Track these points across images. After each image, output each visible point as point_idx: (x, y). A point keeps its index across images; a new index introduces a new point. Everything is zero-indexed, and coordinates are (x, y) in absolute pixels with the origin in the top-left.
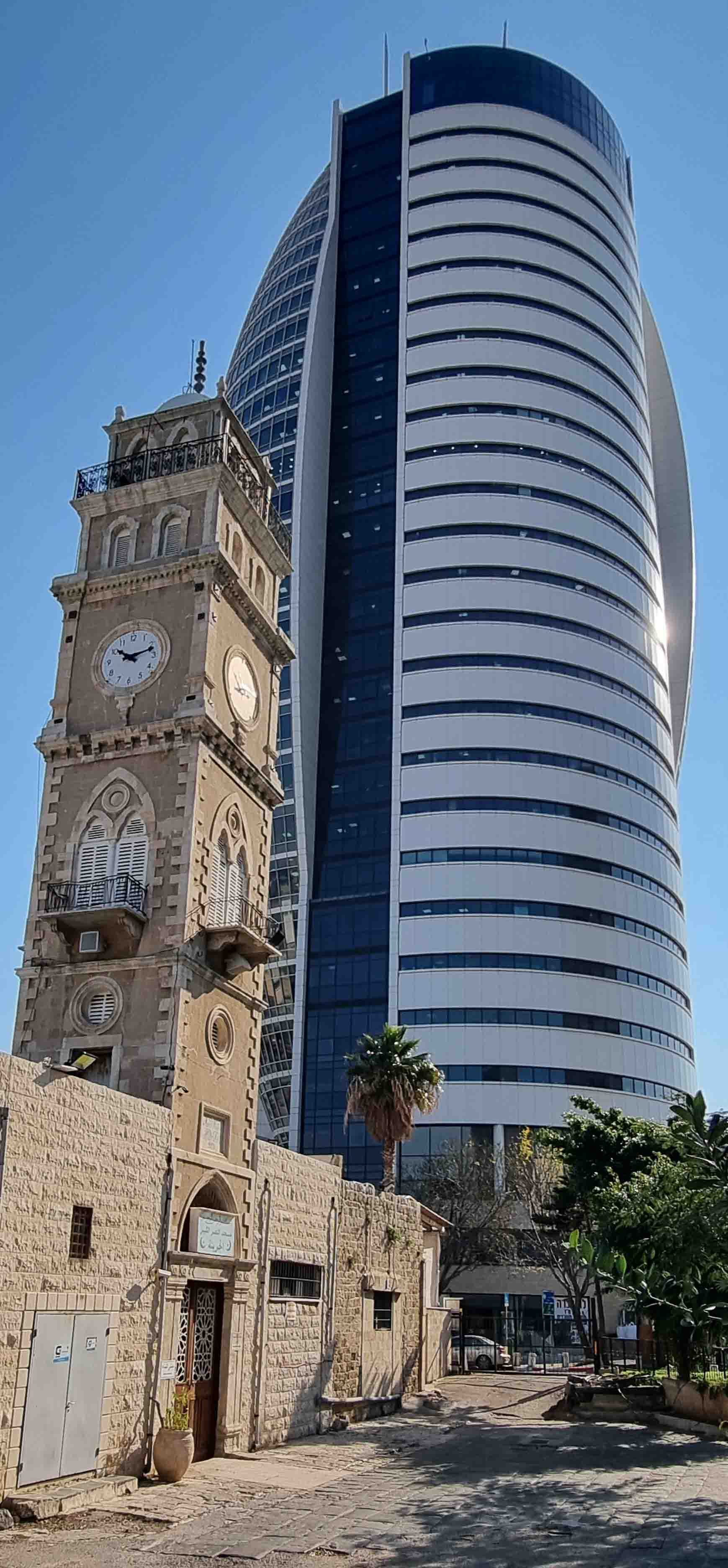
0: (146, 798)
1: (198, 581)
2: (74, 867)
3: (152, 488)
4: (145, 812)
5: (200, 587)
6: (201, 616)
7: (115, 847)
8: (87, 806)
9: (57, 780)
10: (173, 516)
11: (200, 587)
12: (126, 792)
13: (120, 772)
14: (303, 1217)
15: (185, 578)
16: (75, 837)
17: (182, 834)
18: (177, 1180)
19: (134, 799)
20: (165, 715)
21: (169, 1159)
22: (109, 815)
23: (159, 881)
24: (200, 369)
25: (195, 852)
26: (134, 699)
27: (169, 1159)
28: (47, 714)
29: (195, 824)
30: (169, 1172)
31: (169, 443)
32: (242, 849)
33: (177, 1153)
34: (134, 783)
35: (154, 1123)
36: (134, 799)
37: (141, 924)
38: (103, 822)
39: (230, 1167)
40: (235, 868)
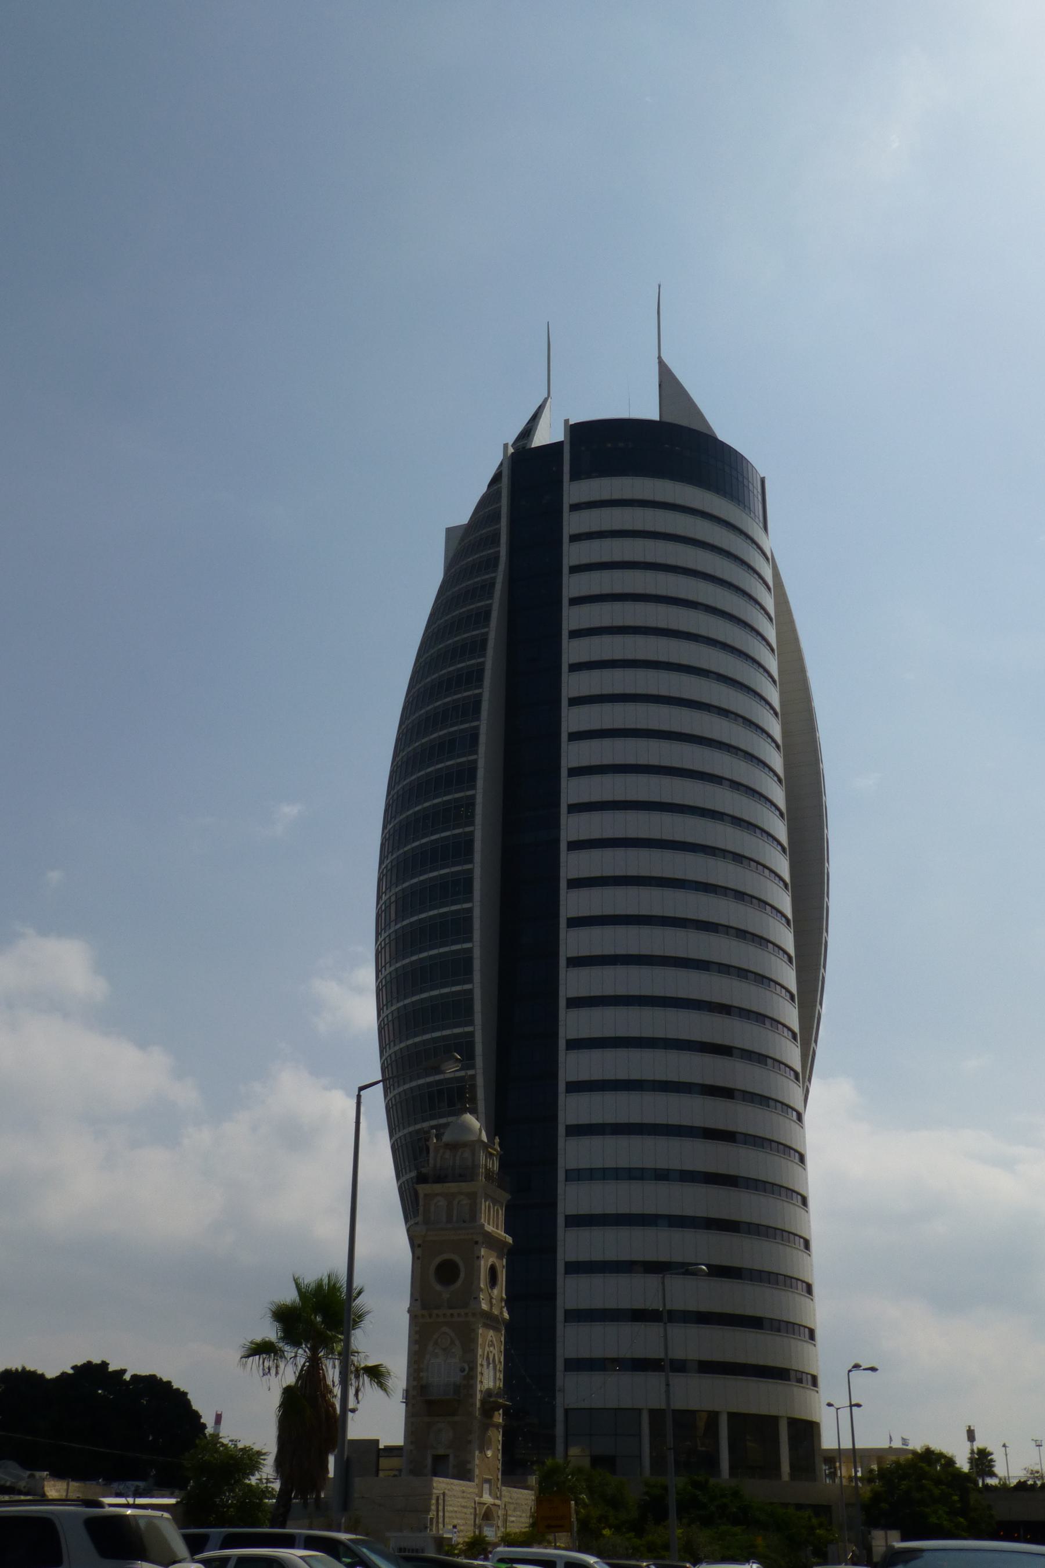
0: (457, 1342)
5: (477, 1243)
6: (478, 1258)
11: (477, 1243)
13: (445, 1329)
35: (471, 1490)
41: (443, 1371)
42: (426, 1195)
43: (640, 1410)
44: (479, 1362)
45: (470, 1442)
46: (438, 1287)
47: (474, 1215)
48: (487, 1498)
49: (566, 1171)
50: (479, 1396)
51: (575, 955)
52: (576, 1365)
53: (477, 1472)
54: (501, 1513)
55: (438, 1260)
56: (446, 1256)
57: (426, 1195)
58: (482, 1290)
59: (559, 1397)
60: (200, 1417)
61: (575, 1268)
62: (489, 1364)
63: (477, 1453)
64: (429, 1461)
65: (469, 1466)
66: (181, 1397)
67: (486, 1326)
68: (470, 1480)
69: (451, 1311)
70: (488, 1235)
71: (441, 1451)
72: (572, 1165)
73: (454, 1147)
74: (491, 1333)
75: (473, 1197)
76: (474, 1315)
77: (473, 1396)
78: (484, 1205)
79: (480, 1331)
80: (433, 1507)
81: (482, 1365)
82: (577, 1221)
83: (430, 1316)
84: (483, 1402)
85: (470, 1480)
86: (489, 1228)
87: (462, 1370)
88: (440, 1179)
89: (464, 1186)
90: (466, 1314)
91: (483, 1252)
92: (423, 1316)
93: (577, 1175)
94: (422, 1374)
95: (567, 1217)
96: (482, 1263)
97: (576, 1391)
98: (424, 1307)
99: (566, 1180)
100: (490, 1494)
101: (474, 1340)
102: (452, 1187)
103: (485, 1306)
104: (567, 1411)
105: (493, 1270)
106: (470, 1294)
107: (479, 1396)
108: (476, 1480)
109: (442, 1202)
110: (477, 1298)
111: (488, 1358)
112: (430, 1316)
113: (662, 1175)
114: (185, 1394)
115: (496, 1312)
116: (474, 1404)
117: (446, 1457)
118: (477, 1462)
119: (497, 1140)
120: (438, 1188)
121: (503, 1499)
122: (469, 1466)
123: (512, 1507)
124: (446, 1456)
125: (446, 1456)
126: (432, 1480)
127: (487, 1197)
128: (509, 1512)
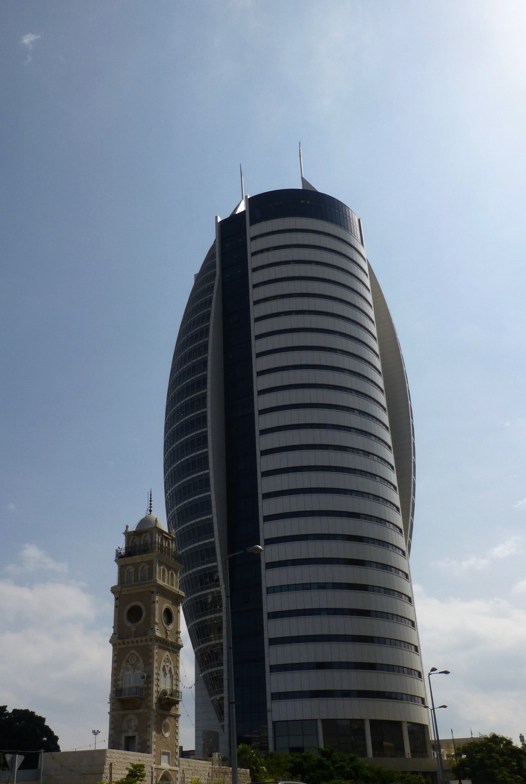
0: (141, 660)
1: (152, 591)
2: (122, 680)
3: (137, 558)
4: (141, 665)
5: (153, 592)
6: (154, 602)
8: (125, 661)
11: (153, 592)
12: (136, 658)
13: (133, 651)
15: (148, 589)
16: (122, 671)
17: (152, 671)
18: (155, 774)
19: (138, 660)
20: (146, 635)
21: (152, 769)
22: (131, 665)
23: (146, 686)
24: (151, 504)
25: (155, 677)
27: (152, 769)
28: (112, 631)
29: (155, 668)
30: (152, 772)
31: (142, 543)
32: (170, 668)
33: (154, 766)
34: (138, 655)
36: (138, 660)
37: (142, 699)
38: (129, 666)
39: (171, 768)
40: (168, 675)
41: (133, 679)
43: (316, 720)
44: (155, 671)
45: (149, 726)
46: (129, 624)
48: (165, 765)
50: (155, 695)
52: (278, 696)
53: (154, 747)
54: (179, 776)
55: (129, 607)
56: (134, 604)
58: (157, 624)
59: (269, 714)
61: (274, 642)
62: (165, 675)
63: (154, 733)
64: (123, 741)
65: (148, 743)
67: (160, 647)
68: (149, 752)
69: (137, 639)
70: (160, 587)
71: (130, 734)
74: (167, 653)
75: (150, 563)
76: (151, 640)
77: (151, 695)
78: (158, 569)
80: (107, 771)
81: (158, 674)
82: (274, 615)
83: (124, 643)
84: (160, 699)
85: (149, 753)
86: (160, 582)
87: (143, 677)
89: (145, 557)
90: (146, 640)
91: (157, 598)
92: (119, 644)
93: (272, 590)
94: (118, 683)
95: (269, 614)
96: (157, 606)
97: (279, 711)
98: (120, 637)
99: (267, 593)
100: (169, 763)
101: (152, 657)
103: (158, 634)
104: (274, 723)
106: (149, 626)
107: (155, 695)
108: (154, 753)
109: (132, 570)
110: (153, 629)
111: (164, 669)
112: (124, 643)
116: (151, 701)
117: (133, 738)
118: (154, 739)
121: (181, 766)
122: (148, 743)
123: (190, 772)
127: (161, 564)
128: (187, 776)
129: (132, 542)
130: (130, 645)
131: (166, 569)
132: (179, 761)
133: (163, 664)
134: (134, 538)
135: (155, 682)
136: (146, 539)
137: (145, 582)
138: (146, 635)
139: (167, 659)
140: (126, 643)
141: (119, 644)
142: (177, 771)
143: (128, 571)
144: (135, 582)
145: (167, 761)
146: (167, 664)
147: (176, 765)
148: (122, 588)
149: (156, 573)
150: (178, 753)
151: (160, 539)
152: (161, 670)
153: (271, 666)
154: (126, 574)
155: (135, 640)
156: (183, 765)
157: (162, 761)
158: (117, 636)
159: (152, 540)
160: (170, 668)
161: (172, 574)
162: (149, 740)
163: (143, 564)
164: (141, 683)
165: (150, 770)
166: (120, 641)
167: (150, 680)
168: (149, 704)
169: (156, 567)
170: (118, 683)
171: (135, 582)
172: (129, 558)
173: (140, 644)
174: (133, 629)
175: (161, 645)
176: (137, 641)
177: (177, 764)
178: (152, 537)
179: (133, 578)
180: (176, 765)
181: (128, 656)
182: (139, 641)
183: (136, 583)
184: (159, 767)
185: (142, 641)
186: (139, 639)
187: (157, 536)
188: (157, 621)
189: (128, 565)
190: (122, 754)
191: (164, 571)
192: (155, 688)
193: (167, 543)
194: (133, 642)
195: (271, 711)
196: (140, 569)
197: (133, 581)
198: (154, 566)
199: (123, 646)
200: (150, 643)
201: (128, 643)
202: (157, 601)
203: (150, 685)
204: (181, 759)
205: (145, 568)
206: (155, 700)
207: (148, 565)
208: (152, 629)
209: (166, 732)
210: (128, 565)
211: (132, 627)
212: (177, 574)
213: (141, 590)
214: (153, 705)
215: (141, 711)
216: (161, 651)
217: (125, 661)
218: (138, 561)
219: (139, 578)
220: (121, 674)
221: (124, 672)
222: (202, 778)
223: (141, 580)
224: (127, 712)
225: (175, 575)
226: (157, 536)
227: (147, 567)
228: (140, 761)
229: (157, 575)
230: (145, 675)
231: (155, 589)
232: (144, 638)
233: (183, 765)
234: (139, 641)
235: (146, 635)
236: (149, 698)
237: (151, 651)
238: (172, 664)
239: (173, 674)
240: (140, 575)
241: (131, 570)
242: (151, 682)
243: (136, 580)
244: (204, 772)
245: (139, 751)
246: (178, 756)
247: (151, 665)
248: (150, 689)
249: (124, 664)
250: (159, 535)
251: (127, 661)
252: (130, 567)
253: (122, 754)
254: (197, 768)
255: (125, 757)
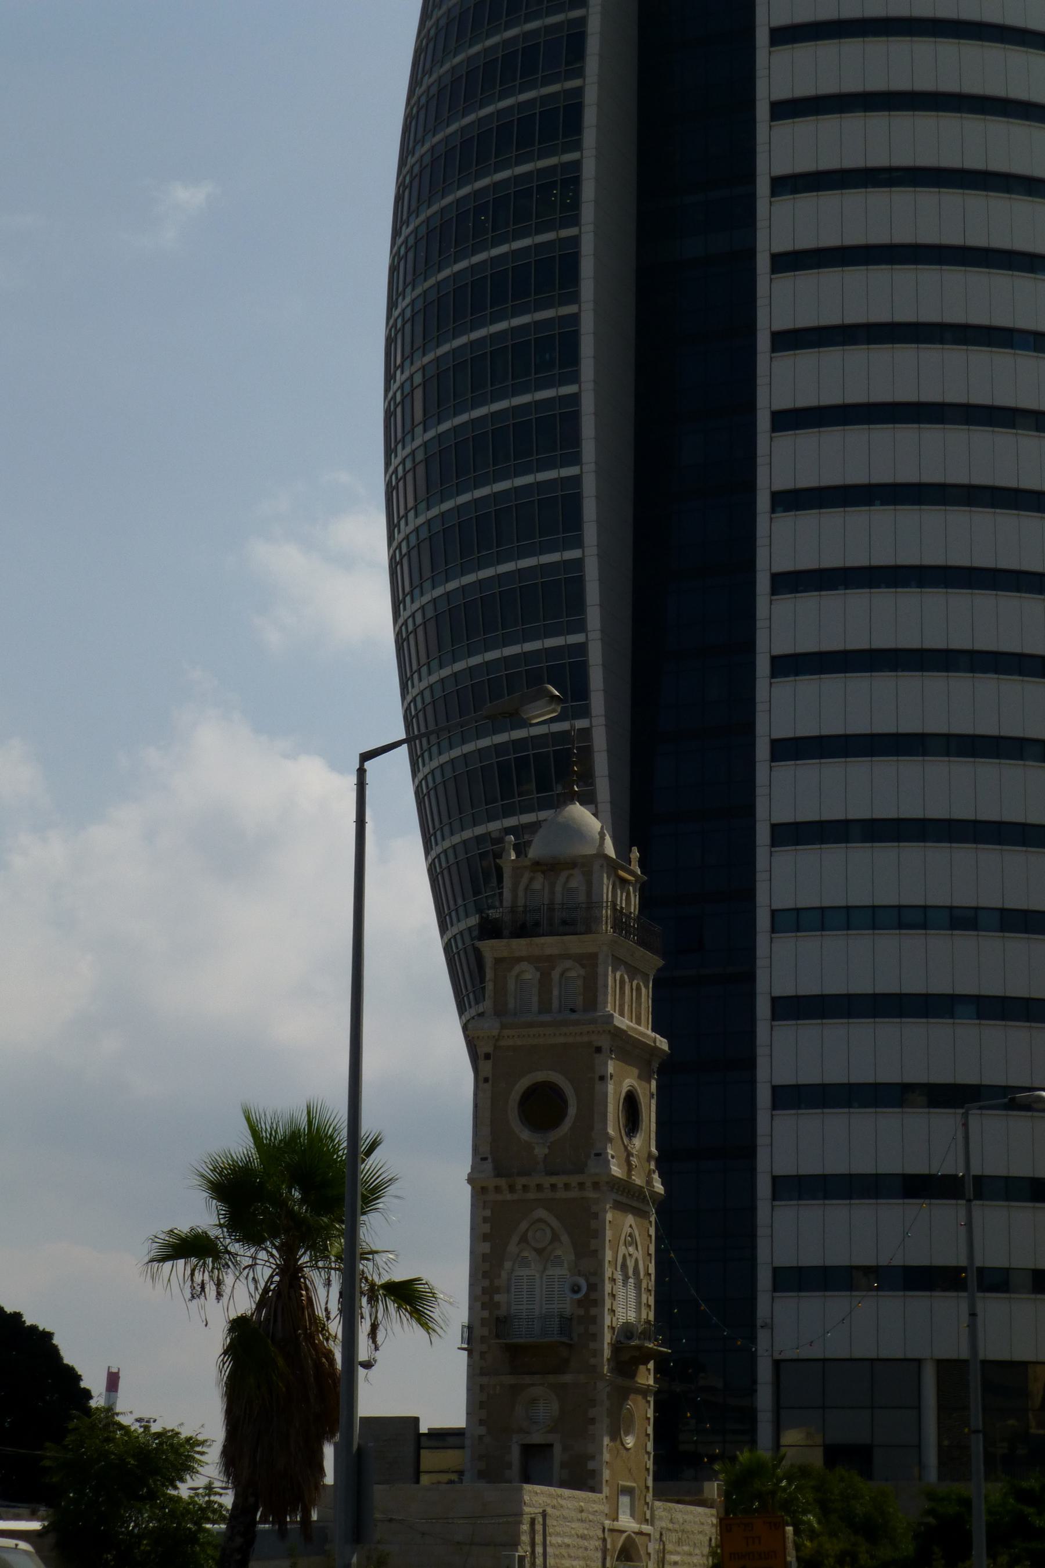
0: (565, 1238)
2: (508, 1291)
4: (565, 1252)
5: (599, 1050)
6: (602, 1078)
7: (541, 1278)
8: (515, 1239)
9: (488, 1213)
10: (568, 970)
11: (599, 1050)
12: (548, 1232)
13: (541, 1213)
14: (687, 1559)
16: (508, 1265)
19: (555, 1238)
23: (581, 1312)
26: (549, 1147)
30: (604, 1540)
35: (596, 1507)
36: (555, 1238)
41: (539, 1290)
42: (498, 961)
43: (919, 1362)
44: (608, 1274)
45: (593, 1421)
46: (525, 1135)
47: (592, 997)
48: (626, 1522)
49: (774, 912)
50: (608, 1337)
51: (789, 485)
52: (795, 1279)
53: (606, 1474)
54: (652, 1547)
56: (540, 1076)
57: (498, 961)
58: (610, 1140)
59: (762, 1336)
60: (79, 1378)
61: (791, 1097)
62: (626, 1278)
63: (606, 1440)
65: (591, 1465)
66: (41, 1343)
67: (619, 1206)
69: (554, 1180)
70: (619, 1034)
71: (537, 1438)
72: (784, 901)
73: (550, 867)
74: (630, 1219)
75: (589, 962)
76: (596, 1185)
77: (597, 1337)
78: (612, 978)
79: (609, 1216)
80: (525, 1538)
81: (613, 1280)
85: (593, 1490)
86: (623, 1022)
87: (575, 1289)
88: (523, 930)
89: (574, 944)
91: (611, 1067)
92: (498, 1189)
93: (794, 920)
94: (497, 1298)
95: (775, 1001)
96: (611, 1088)
97: (793, 1328)
98: (499, 1173)
99: (774, 930)
100: (632, 1515)
101: (598, 1234)
102: (549, 944)
103: (616, 1170)
104: (777, 1364)
105: (631, 1102)
106: (587, 1148)
107: (608, 1337)
108: (606, 1490)
109: (530, 974)
111: (624, 1266)
113: (963, 919)
114: (48, 1336)
115: (638, 1180)
116: (598, 1353)
118: (606, 1456)
119: (635, 854)
120: (520, 946)
122: (591, 1465)
123: (674, 1537)
124: (551, 1446)
125: (551, 1446)
126: (521, 1489)
127: (618, 962)
128: (669, 1547)
129: (526, 889)
130: (531, 1196)
131: (626, 977)
132: (652, 1508)
133: (622, 1250)
134: (531, 880)
135: (608, 1306)
136: (573, 884)
137: (574, 1016)
138: (580, 1169)
139: (630, 1235)
140: (519, 1187)
141: (498, 1189)
142: (649, 1535)
143: (517, 976)
144: (540, 1012)
145: (628, 1511)
146: (631, 1249)
147: (647, 1520)
148: (503, 1026)
149: (606, 994)
150: (651, 1489)
151: (611, 887)
152: (619, 1269)
153: (775, 1179)
154: (511, 985)
155: (547, 1181)
156: (661, 1519)
157: (620, 1511)
158: (488, 1166)
159: (589, 894)
160: (636, 1260)
161: (638, 989)
162: (593, 1458)
163: (568, 964)
164: (567, 1304)
165: (601, 1535)
166: (502, 1182)
167: (593, 1296)
168: (592, 1361)
169: (606, 975)
170: (497, 1298)
171: (540, 1012)
172: (523, 941)
173: (561, 1194)
174: (540, 1151)
175: (619, 1198)
176: (553, 1187)
177: (648, 1516)
178: (589, 884)
179: (535, 999)
180: (647, 1520)
181: (524, 1225)
182: (560, 1185)
183: (546, 1018)
184: (617, 1525)
185: (567, 1187)
186: (559, 1180)
187: (605, 880)
188: (610, 1131)
189: (519, 960)
190: (550, 1495)
191: (622, 983)
192: (607, 1322)
193: (624, 895)
194: (539, 1187)
195: (770, 1326)
196: (555, 975)
197: (535, 1007)
198: (600, 970)
199: (509, 1197)
200: (591, 1194)
201: (525, 1188)
202: (611, 1076)
203: (593, 1311)
204: (657, 1504)
205: (573, 974)
206: (607, 1353)
207: (583, 966)
208: (598, 1155)
209: (627, 1435)
210: (519, 960)
211: (539, 1146)
212: (647, 987)
213: (562, 1040)
214: (603, 1366)
215: (567, 1378)
216: (619, 1214)
217: (515, 1239)
218: (548, 951)
219: (555, 1004)
220: (504, 1275)
221: (513, 1270)
222: (697, 1551)
223: (560, 1011)
224: (527, 1379)
225: (643, 990)
226: (605, 880)
227: (576, 972)
228: (582, 1511)
229: (610, 998)
230: (582, 1282)
231: (604, 1042)
232: (574, 1180)
233: (661, 1519)
234: (560, 1185)
235: (580, 1169)
236: (592, 1345)
237: (596, 1216)
238: (640, 1248)
239: (642, 1276)
240: (556, 992)
241: (527, 976)
242: (598, 1303)
243: (545, 1007)
244: (701, 1537)
245: (563, 1484)
246: (650, 1497)
247: (596, 1255)
248: (595, 1320)
249: (512, 1248)
250: (608, 878)
251: (524, 1239)
252: (524, 966)
253: (550, 1495)
254: (688, 1527)
255: (555, 1502)
